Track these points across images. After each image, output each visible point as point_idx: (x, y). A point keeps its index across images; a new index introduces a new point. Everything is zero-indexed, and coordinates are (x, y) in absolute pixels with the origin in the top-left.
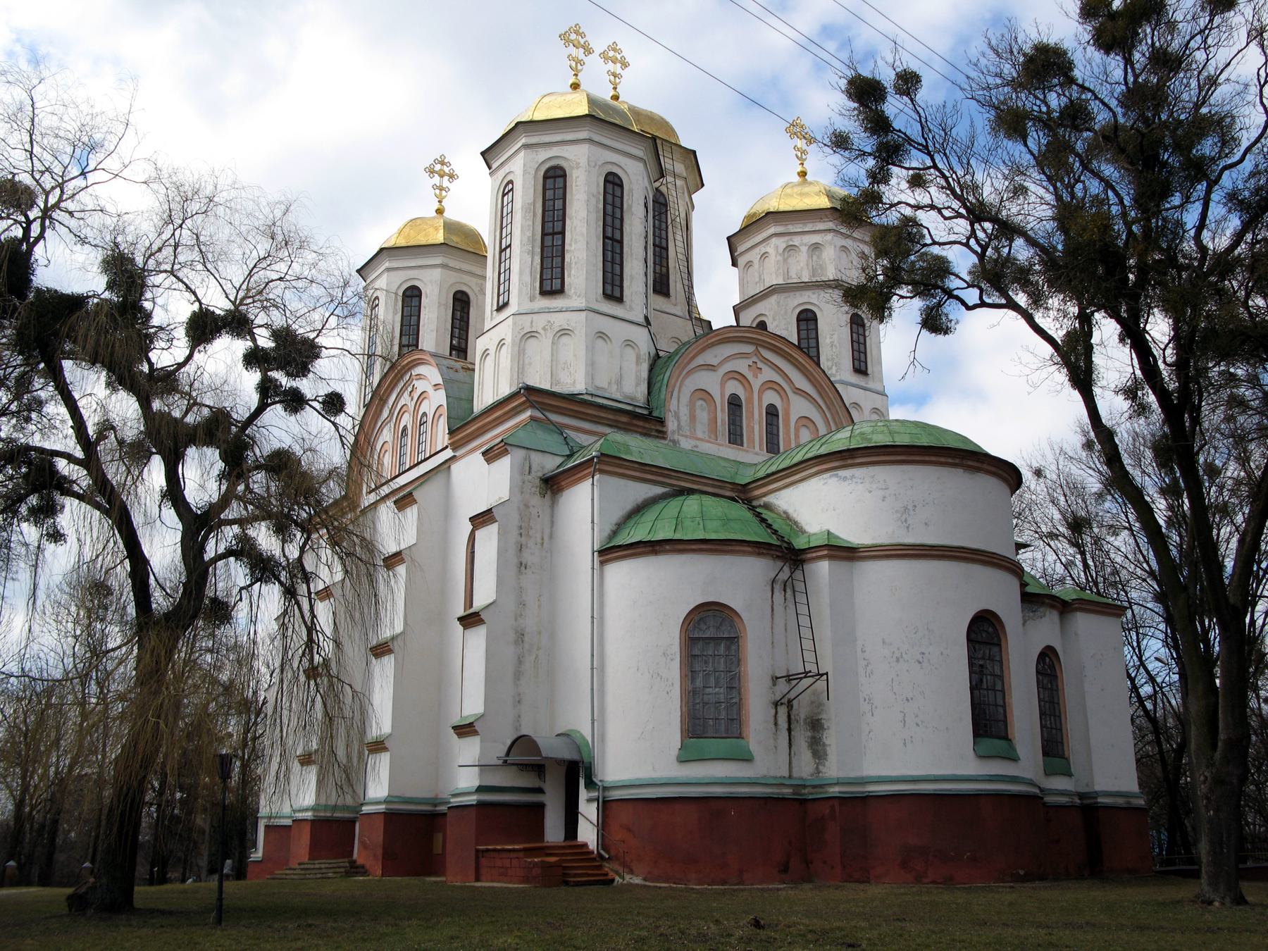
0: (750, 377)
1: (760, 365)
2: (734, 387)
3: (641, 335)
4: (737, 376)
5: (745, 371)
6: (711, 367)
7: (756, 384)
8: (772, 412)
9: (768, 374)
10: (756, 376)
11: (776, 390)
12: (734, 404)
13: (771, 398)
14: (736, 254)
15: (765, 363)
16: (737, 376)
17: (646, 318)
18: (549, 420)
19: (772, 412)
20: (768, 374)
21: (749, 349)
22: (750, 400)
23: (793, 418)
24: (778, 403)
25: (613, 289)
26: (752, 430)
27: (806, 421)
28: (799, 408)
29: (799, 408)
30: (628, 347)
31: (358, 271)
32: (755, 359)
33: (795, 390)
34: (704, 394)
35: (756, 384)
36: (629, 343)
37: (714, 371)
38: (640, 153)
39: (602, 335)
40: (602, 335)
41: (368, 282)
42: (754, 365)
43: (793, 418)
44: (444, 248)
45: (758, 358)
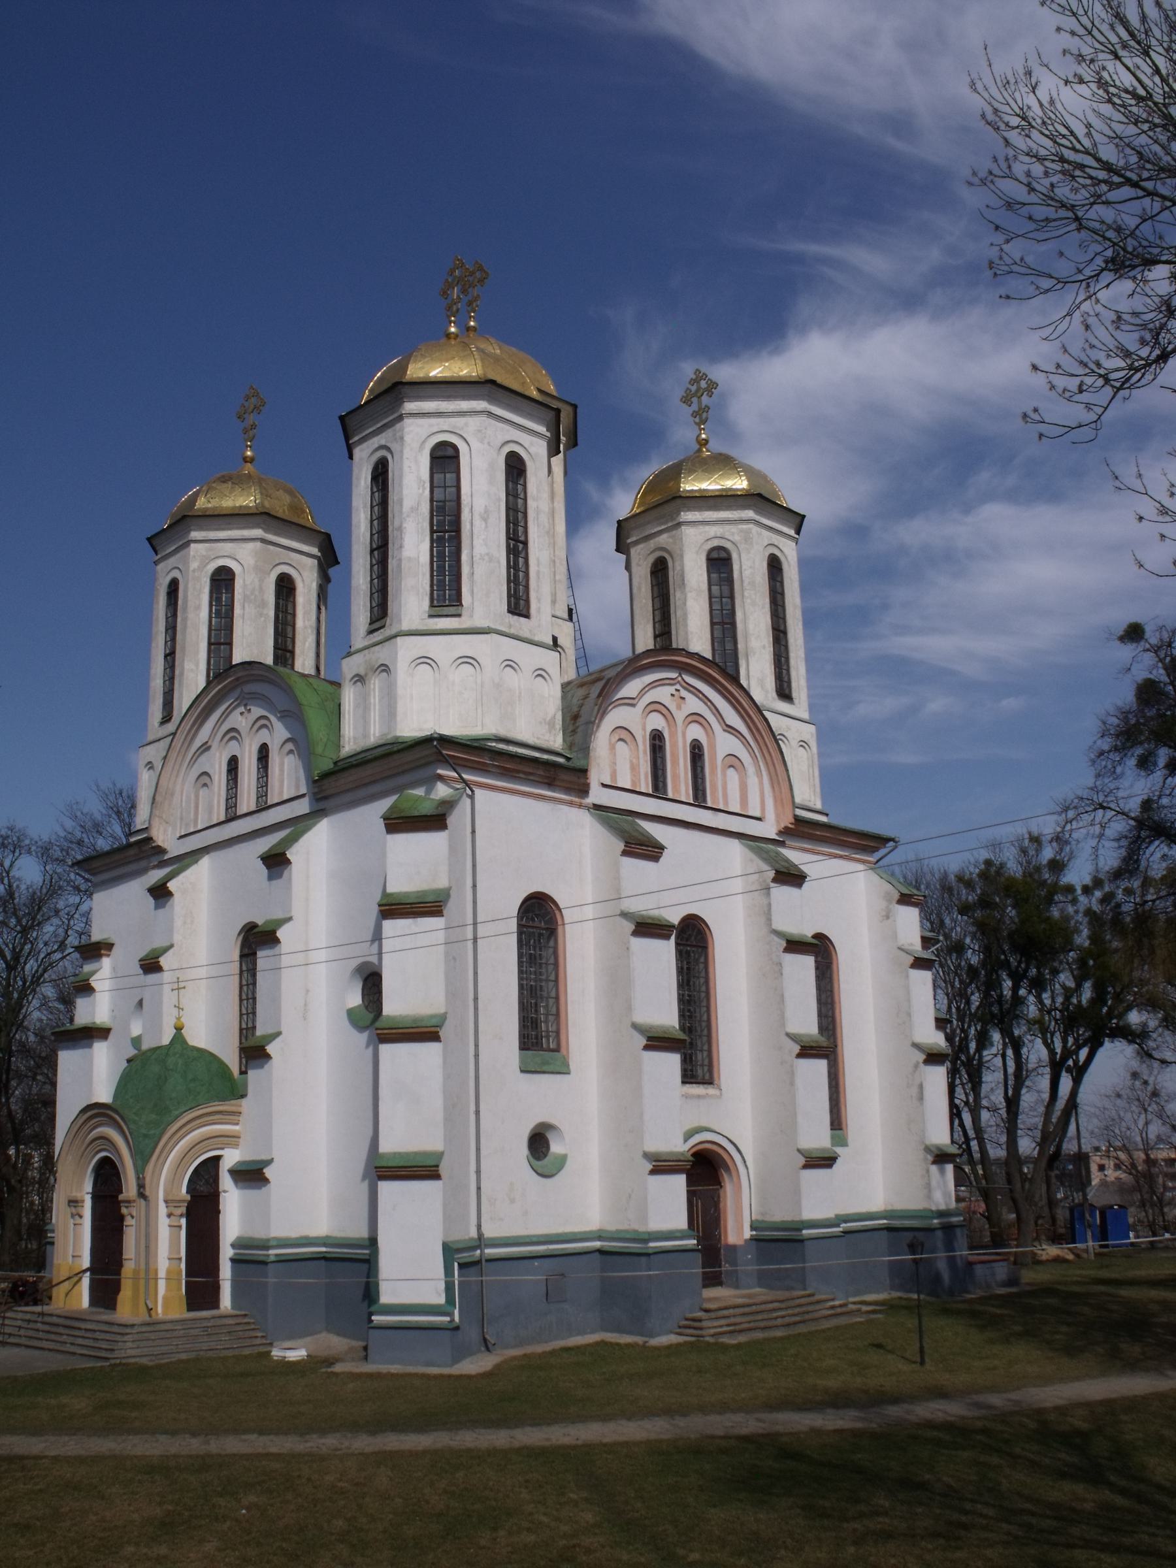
0: (672, 708)
1: (684, 693)
2: (656, 722)
3: (549, 659)
4: (656, 707)
5: (667, 701)
6: (630, 702)
7: (680, 716)
8: (697, 753)
10: (679, 708)
11: (701, 724)
12: (657, 741)
13: (695, 732)
14: (629, 541)
15: (690, 691)
16: (656, 707)
17: (555, 639)
18: (462, 778)
19: (697, 753)
20: (693, 704)
21: (674, 675)
22: (673, 734)
23: (720, 755)
24: (704, 741)
25: (518, 604)
26: (676, 777)
27: (733, 761)
28: (724, 745)
29: (724, 745)
30: (540, 679)
31: (149, 539)
32: (678, 687)
34: (624, 733)
36: (541, 673)
37: (633, 705)
38: (542, 429)
39: (510, 664)
40: (510, 664)
41: (159, 556)
43: (720, 755)
44: (265, 517)
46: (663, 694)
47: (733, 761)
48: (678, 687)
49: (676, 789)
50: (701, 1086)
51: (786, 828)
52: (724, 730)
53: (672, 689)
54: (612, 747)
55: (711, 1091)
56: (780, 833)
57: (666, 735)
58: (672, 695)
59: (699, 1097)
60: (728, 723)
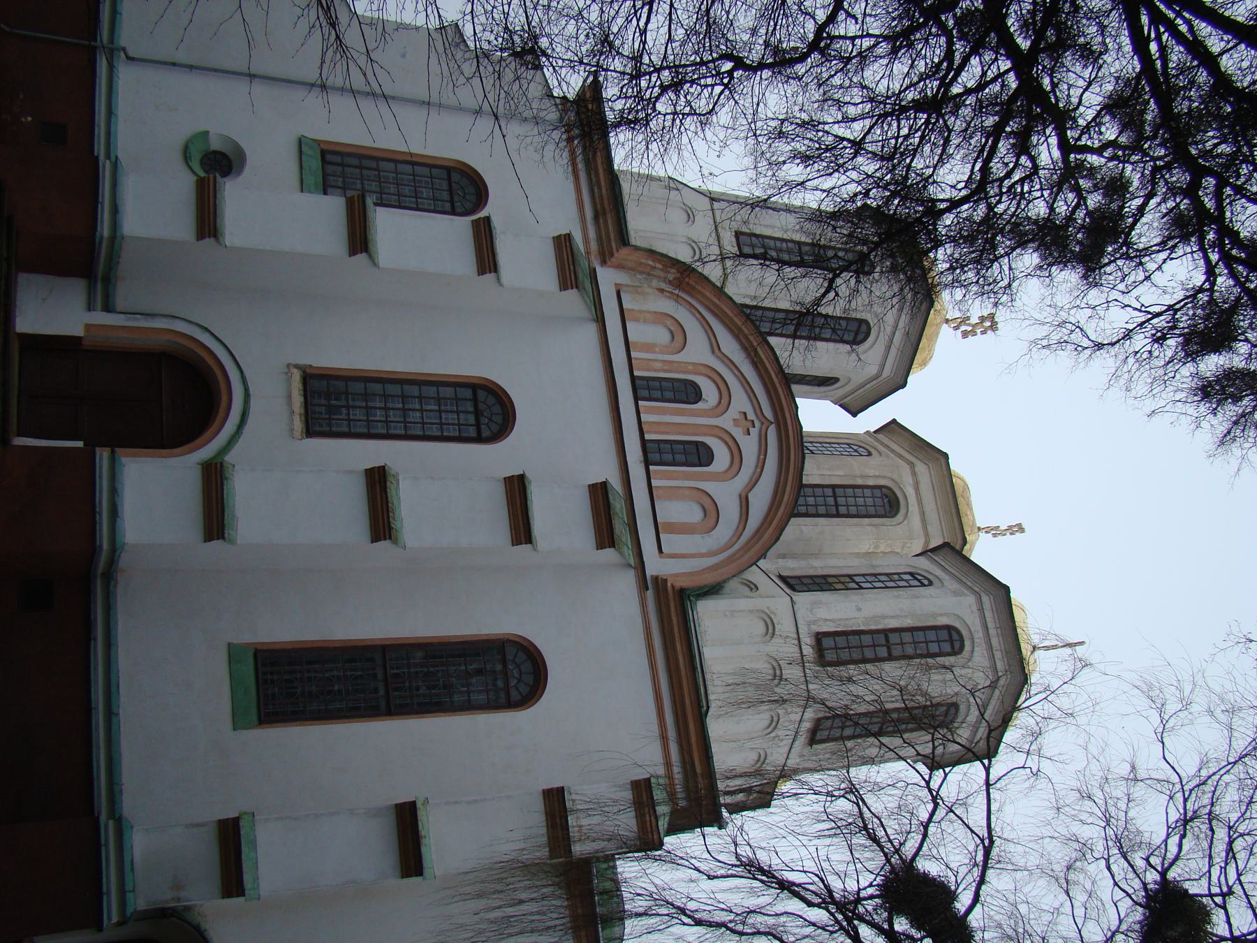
0: (733, 412)
1: (754, 432)
2: (710, 392)
6: (715, 347)
8: (699, 455)
9: (749, 446)
19: (699, 455)
20: (749, 446)
23: (708, 486)
27: (711, 511)
33: (743, 496)
34: (679, 336)
35: (726, 422)
37: (713, 352)
42: (750, 424)
45: (760, 430)
46: (740, 402)
47: (711, 511)
48: (757, 424)
49: (650, 411)
50: (303, 411)
51: (665, 581)
52: (740, 496)
53: (751, 416)
54: (661, 318)
55: (298, 425)
56: (656, 579)
57: (700, 405)
58: (745, 414)
59: (289, 397)
60: (749, 495)
